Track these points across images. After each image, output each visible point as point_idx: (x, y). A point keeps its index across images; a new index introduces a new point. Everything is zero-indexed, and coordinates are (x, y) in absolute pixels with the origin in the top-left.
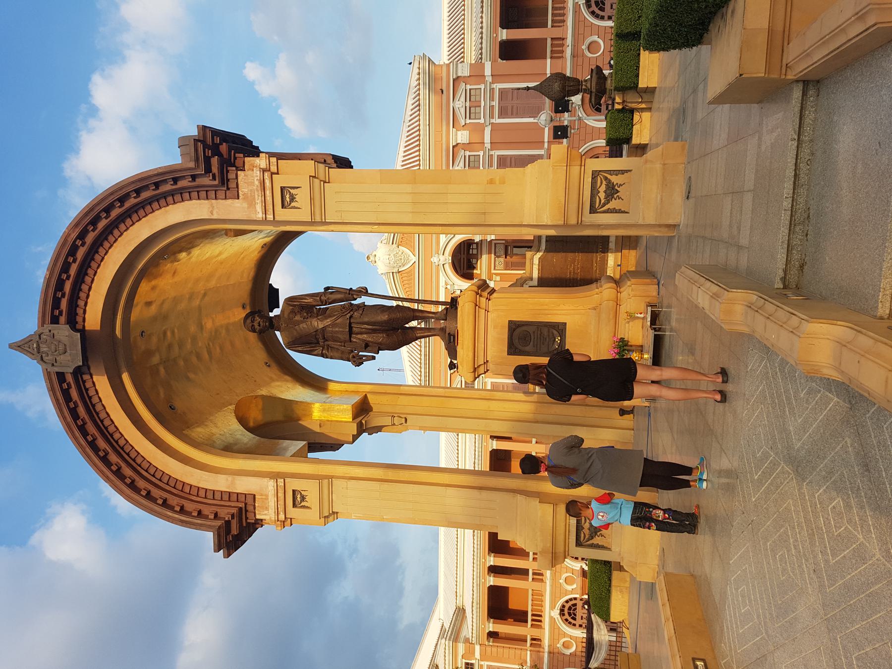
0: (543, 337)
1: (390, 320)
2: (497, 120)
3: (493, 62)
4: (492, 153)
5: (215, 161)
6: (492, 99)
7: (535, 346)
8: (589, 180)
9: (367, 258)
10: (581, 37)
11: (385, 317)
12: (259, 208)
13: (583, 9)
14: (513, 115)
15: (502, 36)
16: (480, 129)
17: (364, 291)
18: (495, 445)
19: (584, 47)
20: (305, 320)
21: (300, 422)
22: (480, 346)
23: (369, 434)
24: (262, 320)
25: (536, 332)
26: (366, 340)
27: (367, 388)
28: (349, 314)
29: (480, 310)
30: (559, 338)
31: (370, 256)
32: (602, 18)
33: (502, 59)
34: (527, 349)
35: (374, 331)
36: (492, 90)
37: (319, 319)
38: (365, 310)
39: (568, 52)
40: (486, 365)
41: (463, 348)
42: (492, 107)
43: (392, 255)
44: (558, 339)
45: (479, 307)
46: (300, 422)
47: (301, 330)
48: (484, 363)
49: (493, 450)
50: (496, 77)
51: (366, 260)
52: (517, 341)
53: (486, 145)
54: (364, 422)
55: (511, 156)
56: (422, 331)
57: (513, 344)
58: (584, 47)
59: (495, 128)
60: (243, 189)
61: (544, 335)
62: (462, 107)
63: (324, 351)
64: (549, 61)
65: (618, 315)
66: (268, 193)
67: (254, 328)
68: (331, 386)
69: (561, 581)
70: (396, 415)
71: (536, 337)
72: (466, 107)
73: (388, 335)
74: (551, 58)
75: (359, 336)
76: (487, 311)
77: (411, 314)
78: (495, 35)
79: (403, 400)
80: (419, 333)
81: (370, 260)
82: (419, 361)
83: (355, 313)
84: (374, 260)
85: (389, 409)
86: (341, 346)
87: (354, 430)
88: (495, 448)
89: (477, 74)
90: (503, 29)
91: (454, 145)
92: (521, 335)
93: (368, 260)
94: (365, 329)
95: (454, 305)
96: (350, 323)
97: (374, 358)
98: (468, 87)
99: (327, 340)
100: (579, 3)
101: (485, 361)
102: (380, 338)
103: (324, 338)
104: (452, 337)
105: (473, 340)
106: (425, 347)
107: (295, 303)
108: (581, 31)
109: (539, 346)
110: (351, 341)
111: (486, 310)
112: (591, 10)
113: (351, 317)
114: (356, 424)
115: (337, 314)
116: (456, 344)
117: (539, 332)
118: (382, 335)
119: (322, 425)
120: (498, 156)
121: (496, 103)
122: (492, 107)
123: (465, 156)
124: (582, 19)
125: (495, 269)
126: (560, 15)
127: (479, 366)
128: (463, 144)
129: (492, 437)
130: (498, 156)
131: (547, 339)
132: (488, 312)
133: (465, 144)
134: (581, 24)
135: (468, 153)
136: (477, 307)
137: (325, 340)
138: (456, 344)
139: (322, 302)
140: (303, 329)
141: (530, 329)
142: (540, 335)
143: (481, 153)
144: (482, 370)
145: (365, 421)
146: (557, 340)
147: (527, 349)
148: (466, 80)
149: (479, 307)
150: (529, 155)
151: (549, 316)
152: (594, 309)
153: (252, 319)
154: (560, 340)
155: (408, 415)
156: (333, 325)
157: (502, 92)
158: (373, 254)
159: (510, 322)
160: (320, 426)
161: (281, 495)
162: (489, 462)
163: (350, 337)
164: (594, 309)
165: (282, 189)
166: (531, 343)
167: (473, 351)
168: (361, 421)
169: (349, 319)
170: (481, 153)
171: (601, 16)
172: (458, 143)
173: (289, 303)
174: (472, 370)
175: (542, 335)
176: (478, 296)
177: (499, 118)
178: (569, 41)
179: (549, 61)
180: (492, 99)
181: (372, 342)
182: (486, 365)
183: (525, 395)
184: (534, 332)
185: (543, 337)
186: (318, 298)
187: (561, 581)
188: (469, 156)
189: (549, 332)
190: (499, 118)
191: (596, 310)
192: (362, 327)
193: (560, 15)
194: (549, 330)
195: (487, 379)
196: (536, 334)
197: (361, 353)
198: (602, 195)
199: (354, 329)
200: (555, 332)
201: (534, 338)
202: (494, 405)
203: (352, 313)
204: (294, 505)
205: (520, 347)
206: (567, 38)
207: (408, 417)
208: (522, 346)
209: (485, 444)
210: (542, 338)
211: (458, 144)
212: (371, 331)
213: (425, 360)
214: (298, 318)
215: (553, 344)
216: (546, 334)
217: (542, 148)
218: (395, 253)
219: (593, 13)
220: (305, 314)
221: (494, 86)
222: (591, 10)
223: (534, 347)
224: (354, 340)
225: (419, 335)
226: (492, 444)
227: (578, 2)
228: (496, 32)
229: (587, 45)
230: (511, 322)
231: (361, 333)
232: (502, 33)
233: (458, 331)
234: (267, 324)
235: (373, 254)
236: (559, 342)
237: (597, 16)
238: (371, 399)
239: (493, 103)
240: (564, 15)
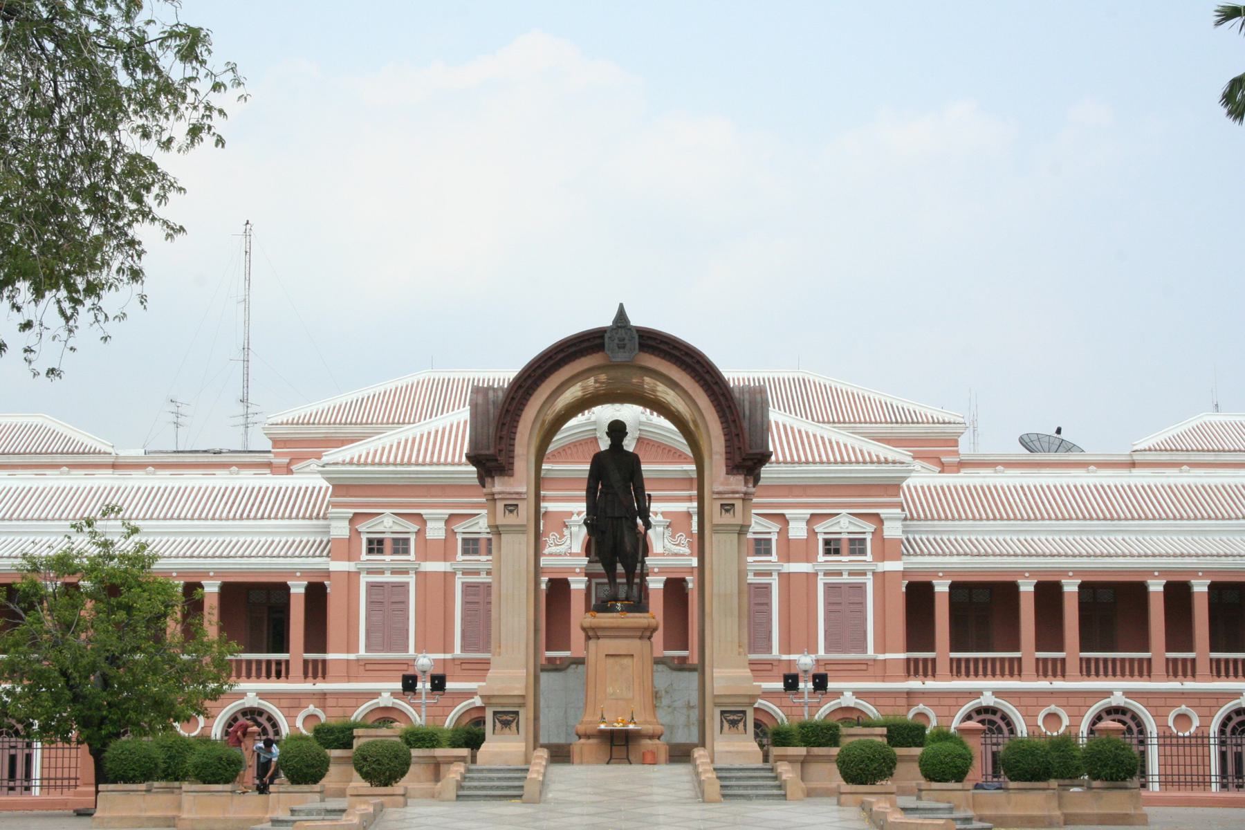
2: (821, 581)
3: (904, 573)
4: (775, 576)
5: (749, 463)
6: (851, 573)
8: (741, 709)
10: (935, 701)
12: (721, 489)
14: (828, 604)
15: (940, 585)
16: (809, 557)
19: (921, 706)
33: (907, 587)
36: (864, 573)
39: (915, 684)
42: (840, 574)
50: (881, 577)
58: (921, 706)
59: (811, 577)
60: (732, 478)
62: (841, 528)
64: (903, 656)
66: (731, 495)
69: (311, 707)
72: (840, 533)
74: (908, 660)
88: (292, 591)
89: (886, 549)
98: (869, 537)
108: (944, 701)
121: (845, 579)
122: (840, 574)
125: (597, 584)
126: (985, 669)
135: (774, 537)
148: (878, 533)
150: (770, 632)
157: (861, 588)
161: (514, 496)
165: (733, 505)
172: (788, 522)
177: (825, 584)
178: (931, 684)
179: (903, 656)
180: (851, 573)
187: (311, 707)
190: (825, 584)
193: (985, 669)
195: (414, 576)
198: (731, 718)
204: (505, 505)
217: (782, 651)
221: (870, 576)
226: (298, 586)
229: (924, 711)
239: (845, 576)
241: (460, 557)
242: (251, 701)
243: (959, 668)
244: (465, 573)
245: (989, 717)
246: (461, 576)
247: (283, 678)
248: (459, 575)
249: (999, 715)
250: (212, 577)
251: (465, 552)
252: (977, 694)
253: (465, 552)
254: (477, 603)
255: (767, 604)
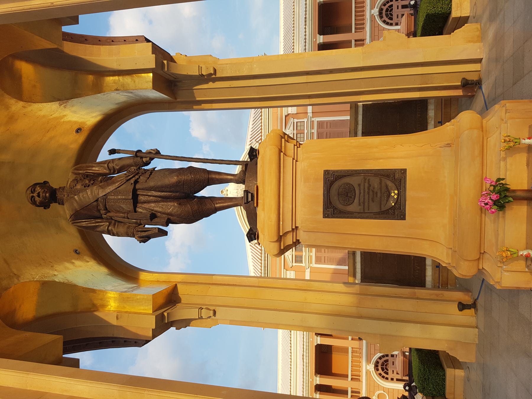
0: (373, 191)
1: (178, 182)
4: (313, 119)
7: (362, 204)
9: (221, 192)
11: (174, 179)
13: (378, 19)
15: (320, 40)
17: (157, 154)
18: (319, 340)
20: (86, 188)
21: (96, 313)
22: (287, 206)
23: (176, 329)
24: (43, 190)
25: (362, 185)
26: (153, 210)
27: (179, 278)
28: (134, 178)
29: (286, 158)
30: (396, 192)
31: (224, 191)
32: (391, 24)
34: (351, 208)
35: (165, 199)
37: (100, 186)
38: (153, 173)
40: (295, 233)
41: (263, 210)
43: (239, 190)
44: (394, 194)
45: (285, 154)
46: (96, 313)
47: (80, 199)
48: (293, 229)
49: (318, 345)
51: (221, 193)
52: (336, 198)
53: (309, 114)
54: (166, 314)
55: (327, 122)
56: (222, 201)
57: (330, 202)
61: (374, 188)
63: (110, 228)
65: (485, 151)
67: (34, 200)
68: (143, 276)
70: (204, 307)
71: (362, 191)
73: (180, 204)
75: (146, 206)
76: (295, 160)
77: (205, 176)
78: (315, 40)
79: (214, 290)
80: (219, 203)
81: (224, 194)
82: (260, 272)
83: (141, 178)
84: (226, 193)
85: (199, 301)
86: (124, 218)
87: (151, 323)
88: (319, 343)
90: (321, 35)
91: (286, 114)
92: (341, 190)
93: (222, 193)
94: (153, 196)
95: (253, 155)
96: (135, 191)
97: (165, 233)
99: (109, 212)
100: (374, 15)
101: (294, 227)
102: (171, 207)
103: (106, 209)
104: (250, 195)
105: (277, 197)
106: (265, 260)
107: (80, 172)
108: (376, 34)
109: (366, 204)
110: (135, 211)
111: (294, 159)
112: (383, 19)
113: (136, 182)
114: (154, 316)
115: (121, 180)
116: (255, 205)
117: (367, 185)
118: (172, 204)
119: (119, 317)
120: (317, 121)
123: (294, 122)
124: (376, 25)
127: (286, 234)
128: (292, 114)
129: (317, 334)
130: (317, 121)
131: (379, 194)
132: (297, 161)
133: (294, 114)
134: (376, 29)
136: (282, 154)
137: (107, 210)
138: (255, 205)
139: (110, 170)
140: (82, 198)
141: (354, 181)
142: (369, 189)
143: (305, 120)
144: (289, 240)
145: (168, 314)
146: (393, 194)
147: (351, 208)
149: (285, 154)
150: (340, 120)
151: (381, 160)
152: (449, 145)
153: (33, 190)
154: (398, 194)
155: (217, 308)
156: (115, 192)
158: (226, 190)
159: (327, 173)
160: (117, 318)
162: (314, 354)
163: (135, 206)
164: (449, 145)
166: (356, 200)
167: (276, 212)
168: (162, 314)
169: (133, 184)
170: (305, 120)
171: (390, 23)
173: (76, 171)
174: (275, 239)
175: (371, 188)
176: (283, 140)
181: (160, 212)
182: (295, 233)
183: (345, 286)
184: (359, 185)
185: (373, 191)
186: (106, 165)
188: (297, 122)
189: (381, 183)
191: (450, 146)
192: (149, 194)
194: (381, 180)
196: (362, 187)
197: (147, 226)
199: (141, 198)
200: (390, 184)
201: (360, 193)
202: (311, 297)
203: (137, 177)
205: (340, 207)
206: (366, 39)
207: (218, 309)
208: (344, 205)
209: (311, 340)
210: (371, 193)
211: (288, 114)
212: (160, 199)
213: (265, 271)
214: (79, 186)
215: (387, 200)
216: (376, 187)
218: (242, 188)
219: (384, 22)
220: (87, 182)
222: (383, 19)
223: (360, 205)
224: (140, 210)
225: (218, 205)
226: (317, 340)
227: (373, 14)
228: (315, 37)
230: (327, 173)
231: (149, 202)
232: (320, 38)
233: (257, 187)
234: (47, 195)
235: (226, 190)
236: (396, 197)
237: (387, 24)
238: (181, 290)
240: (363, 24)
241: (303, 265)
242: (371, 367)
243: (360, 29)
244: (310, 262)
245: (384, 12)
246: (312, 264)
247: (360, 378)
248: (312, 265)
249: (383, 7)
250: (312, 380)
251: (301, 262)
252: (372, 17)
253: (301, 262)
254: (325, 257)
255: (327, 123)
